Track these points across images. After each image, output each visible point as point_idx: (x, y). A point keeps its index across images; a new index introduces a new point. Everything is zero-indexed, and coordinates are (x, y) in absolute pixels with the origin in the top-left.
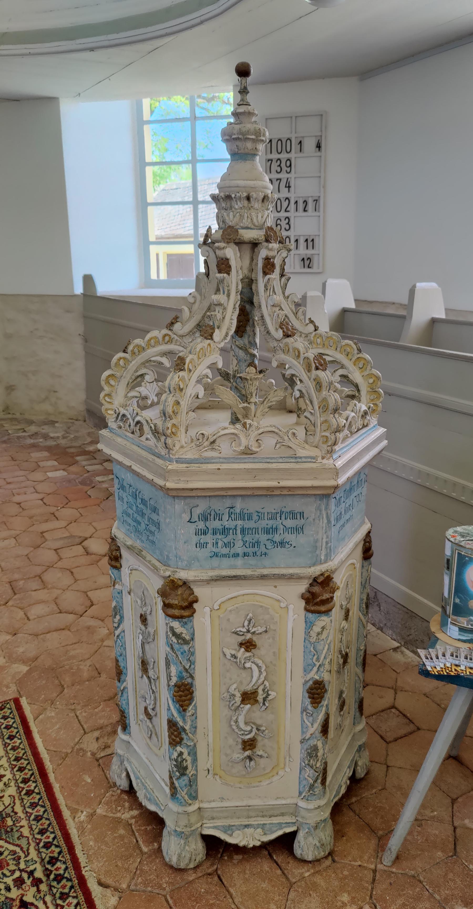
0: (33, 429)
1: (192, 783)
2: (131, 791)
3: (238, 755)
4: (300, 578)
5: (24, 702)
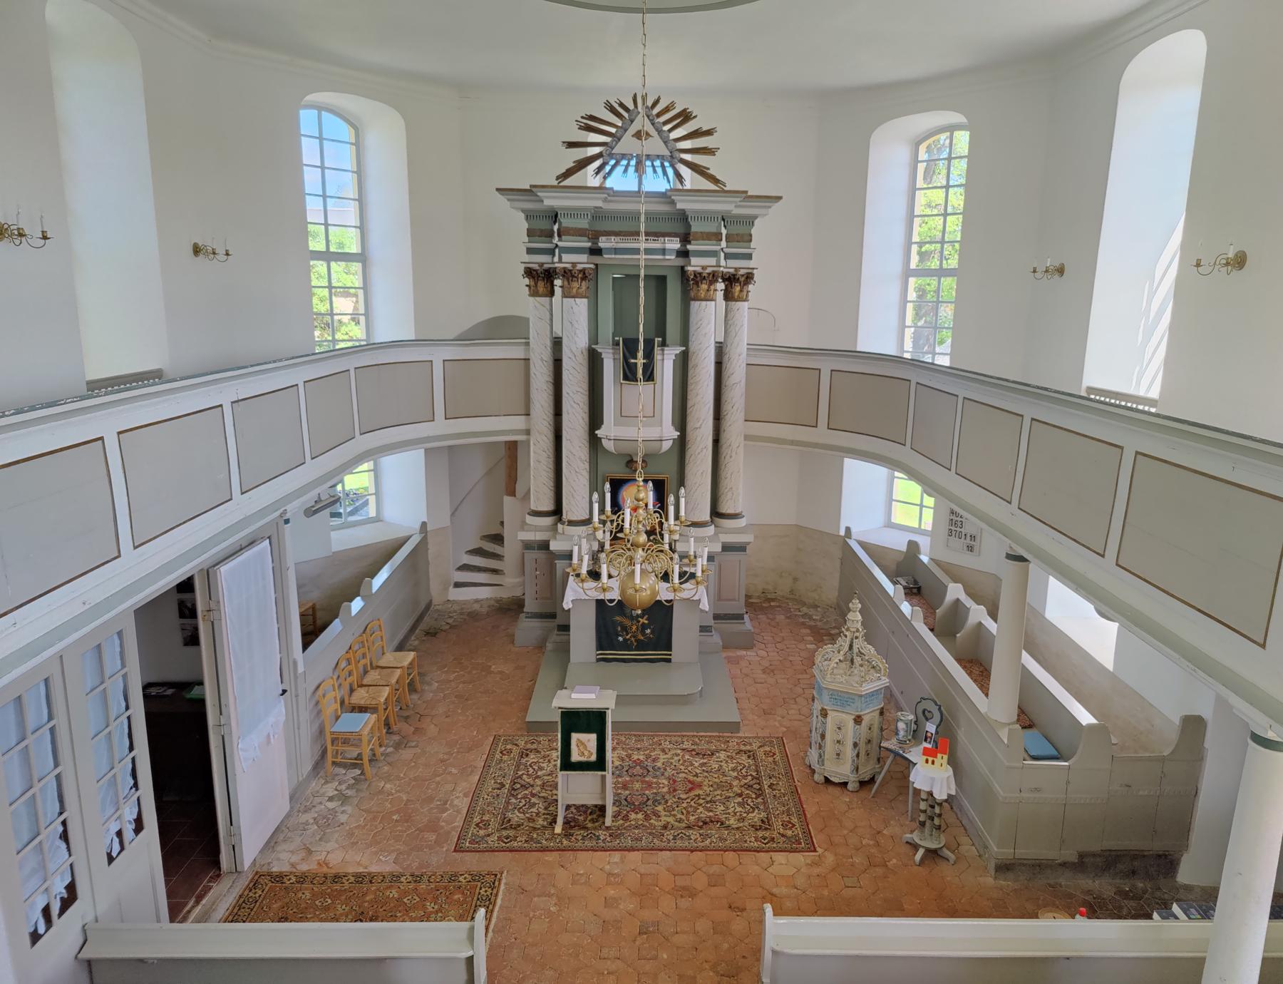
1: (823, 761)
3: (835, 757)
5: (784, 738)
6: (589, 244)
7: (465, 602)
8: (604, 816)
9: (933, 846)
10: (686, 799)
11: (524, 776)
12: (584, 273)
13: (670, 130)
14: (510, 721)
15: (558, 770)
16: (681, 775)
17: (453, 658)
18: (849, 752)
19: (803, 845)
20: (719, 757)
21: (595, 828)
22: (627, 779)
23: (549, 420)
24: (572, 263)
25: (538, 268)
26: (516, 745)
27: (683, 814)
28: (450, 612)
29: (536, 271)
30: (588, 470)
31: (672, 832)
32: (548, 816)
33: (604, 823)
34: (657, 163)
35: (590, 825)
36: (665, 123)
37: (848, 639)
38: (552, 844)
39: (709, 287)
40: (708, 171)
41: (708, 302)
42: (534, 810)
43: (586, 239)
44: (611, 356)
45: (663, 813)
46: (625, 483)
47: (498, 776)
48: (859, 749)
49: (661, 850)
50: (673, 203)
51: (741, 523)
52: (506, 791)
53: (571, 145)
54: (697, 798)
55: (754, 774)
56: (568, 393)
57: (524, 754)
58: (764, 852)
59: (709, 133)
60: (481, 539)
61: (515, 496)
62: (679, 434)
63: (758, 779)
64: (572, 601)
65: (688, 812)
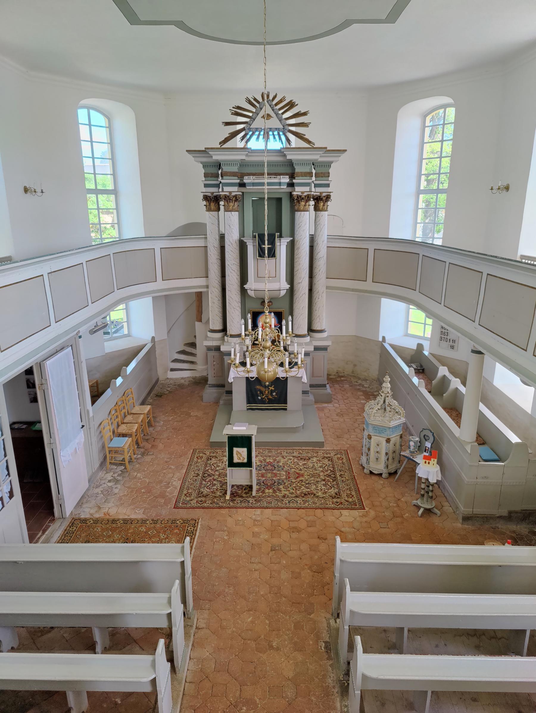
0: (360, 382)
1: (369, 462)
2: (362, 465)
4: (385, 438)
5: (348, 451)
6: (238, 181)
7: (176, 379)
8: (252, 491)
9: (428, 506)
10: (295, 482)
11: (210, 470)
12: (236, 198)
13: (283, 113)
14: (201, 442)
15: (227, 467)
16: (293, 470)
17: (171, 408)
18: (383, 458)
19: (358, 506)
20: (313, 460)
21: (247, 497)
22: (264, 472)
23: (218, 280)
24: (229, 192)
25: (210, 195)
26: (205, 454)
27: (293, 490)
28: (169, 385)
29: (210, 197)
30: (240, 307)
31: (288, 499)
32: (222, 491)
33: (252, 494)
34: (276, 133)
35: (244, 495)
36: (280, 109)
37: (383, 398)
38: (224, 505)
39: (306, 204)
40: (305, 136)
41: (305, 212)
42: (215, 487)
43: (236, 178)
44: (252, 244)
45: (283, 489)
46: (260, 314)
47: (196, 470)
48: (389, 456)
49: (282, 508)
50: (285, 156)
51: (325, 335)
52: (200, 477)
53: (227, 124)
54: (301, 482)
55: (332, 469)
56: (228, 265)
57: (209, 459)
58: (337, 509)
59: (305, 114)
60: (184, 346)
61: (202, 322)
62: (289, 286)
63: (333, 472)
64: (233, 378)
65: (296, 489)
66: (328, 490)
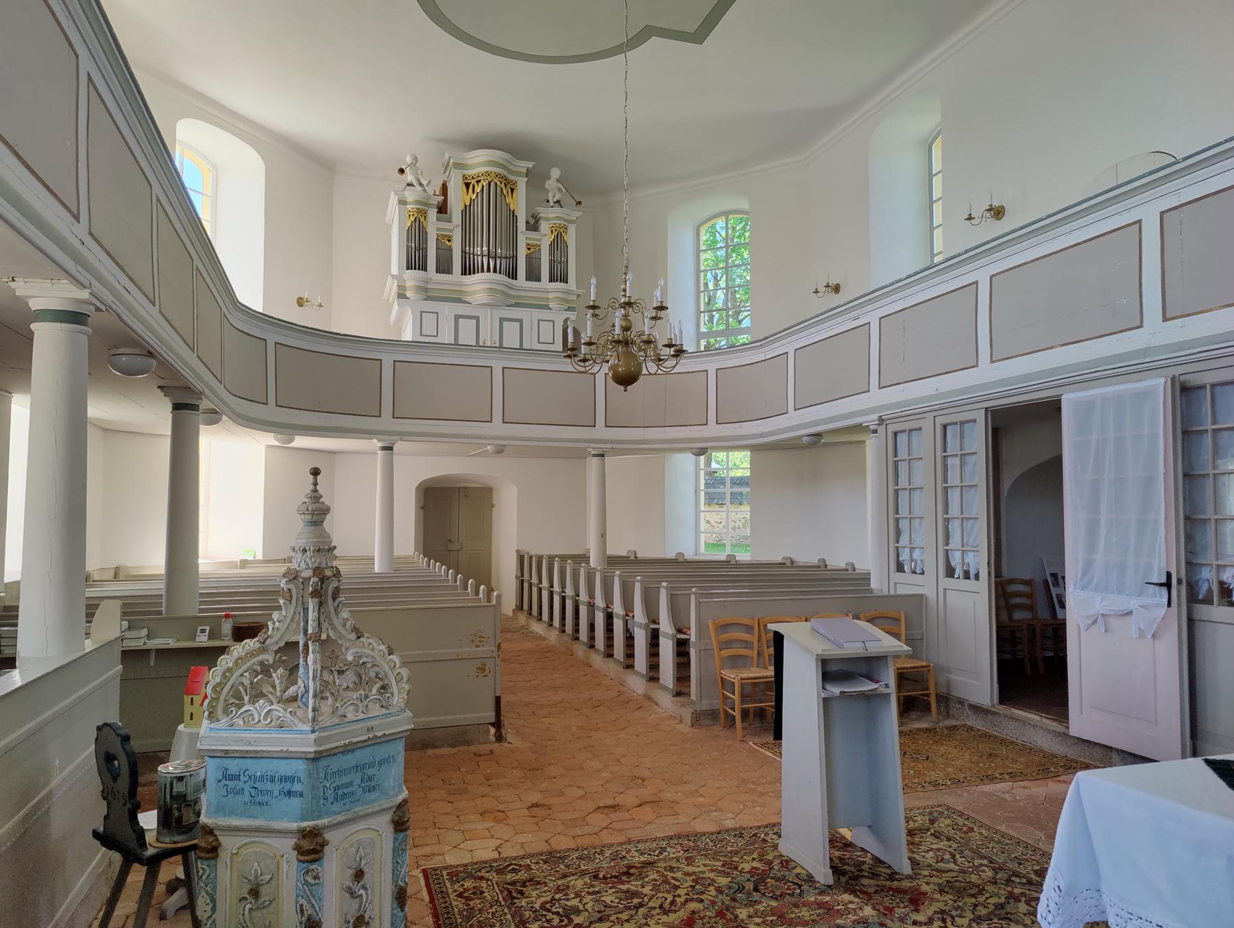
66: (553, 899)
